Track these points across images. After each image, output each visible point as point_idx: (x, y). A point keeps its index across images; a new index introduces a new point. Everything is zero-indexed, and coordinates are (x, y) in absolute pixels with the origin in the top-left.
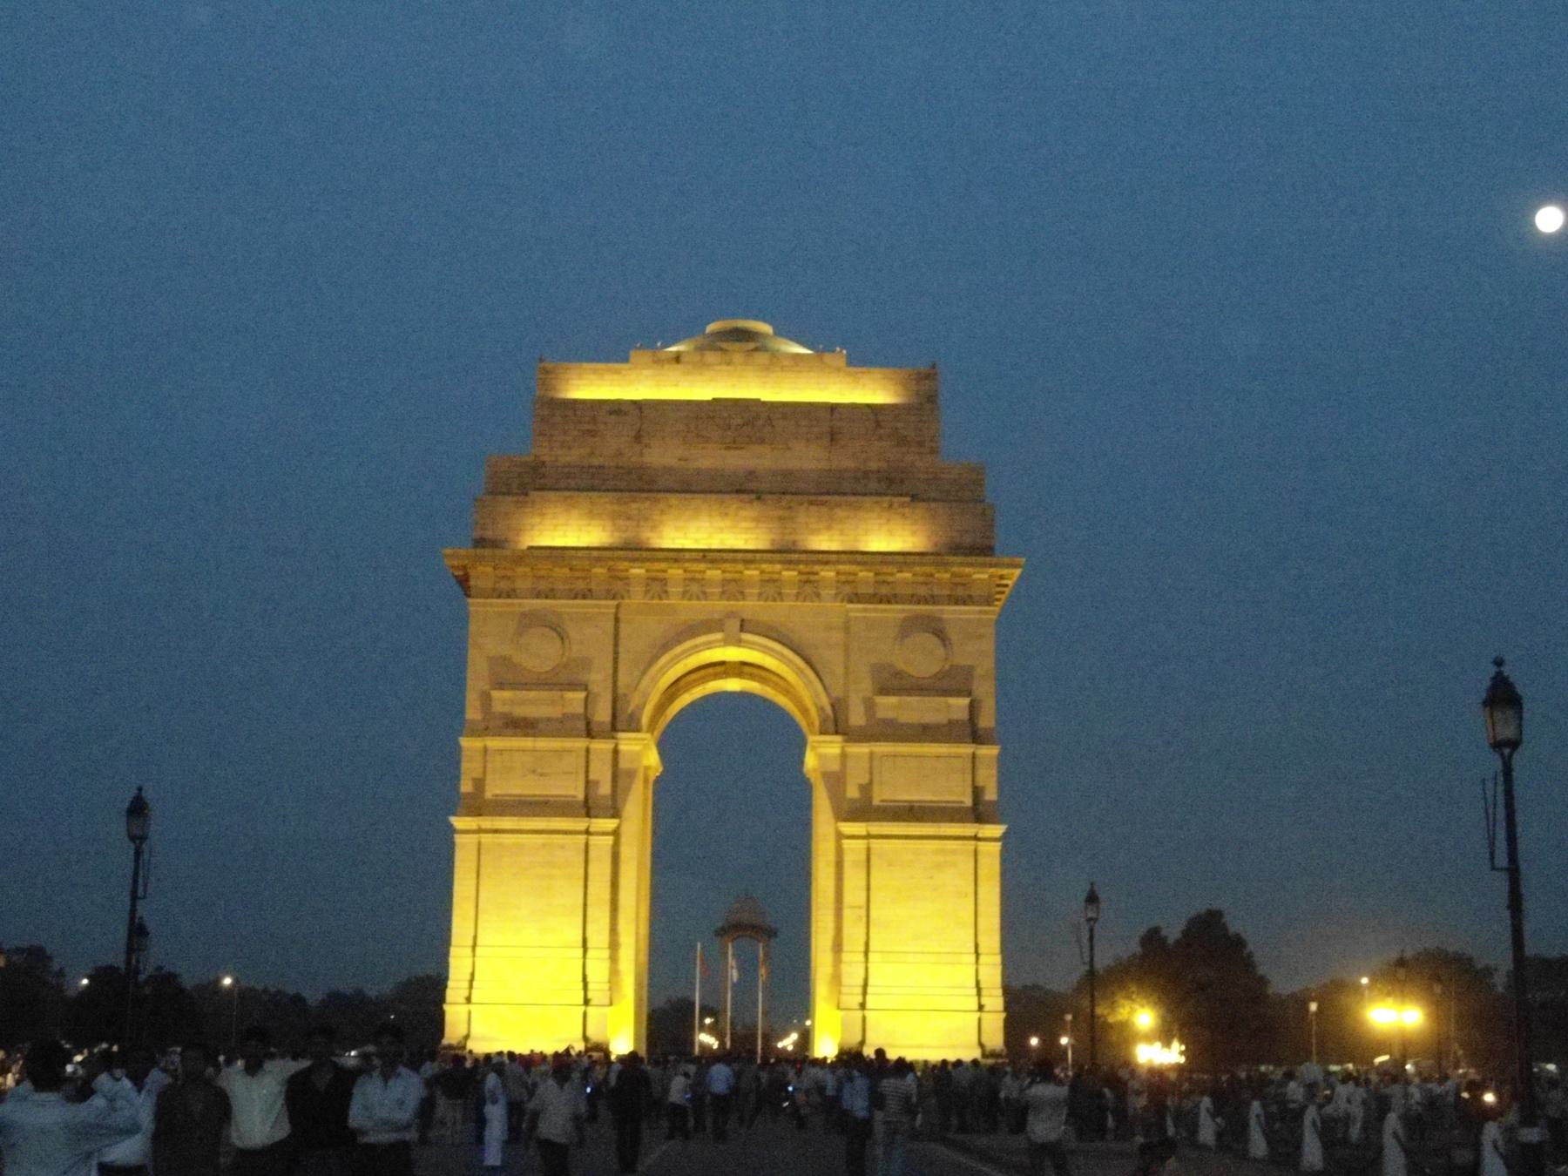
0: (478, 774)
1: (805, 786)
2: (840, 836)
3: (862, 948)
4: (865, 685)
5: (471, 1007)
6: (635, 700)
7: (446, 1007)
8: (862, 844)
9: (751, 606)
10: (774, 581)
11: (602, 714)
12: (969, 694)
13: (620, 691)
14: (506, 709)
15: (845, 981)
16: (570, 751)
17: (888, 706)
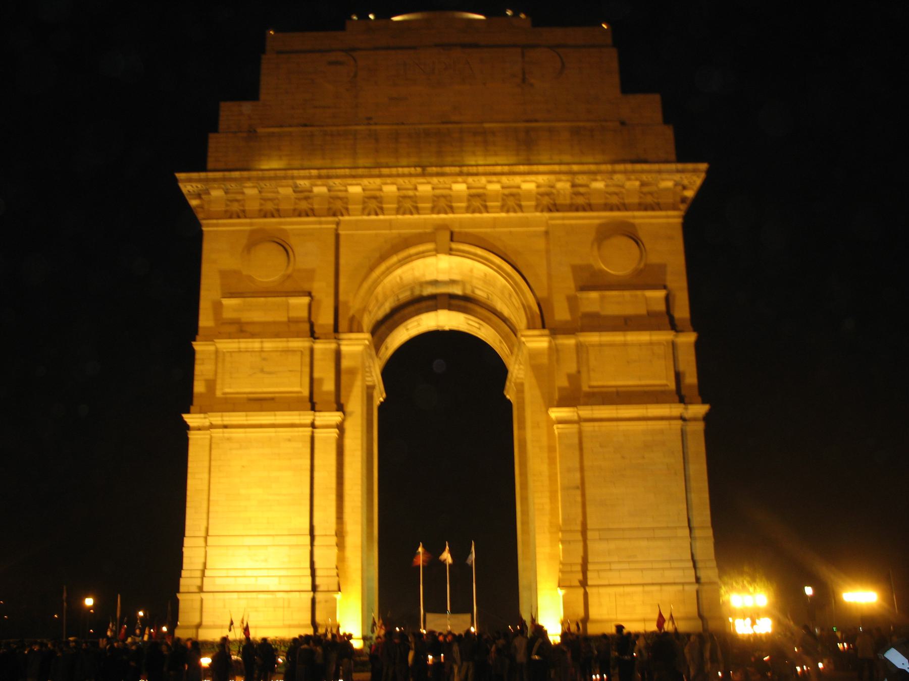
0: (210, 376)
3: (579, 528)
4: (566, 284)
5: (203, 595)
7: (180, 596)
8: (574, 428)
9: (459, 218)
10: (479, 196)
11: (325, 318)
12: (665, 287)
13: (342, 298)
17: (592, 300)
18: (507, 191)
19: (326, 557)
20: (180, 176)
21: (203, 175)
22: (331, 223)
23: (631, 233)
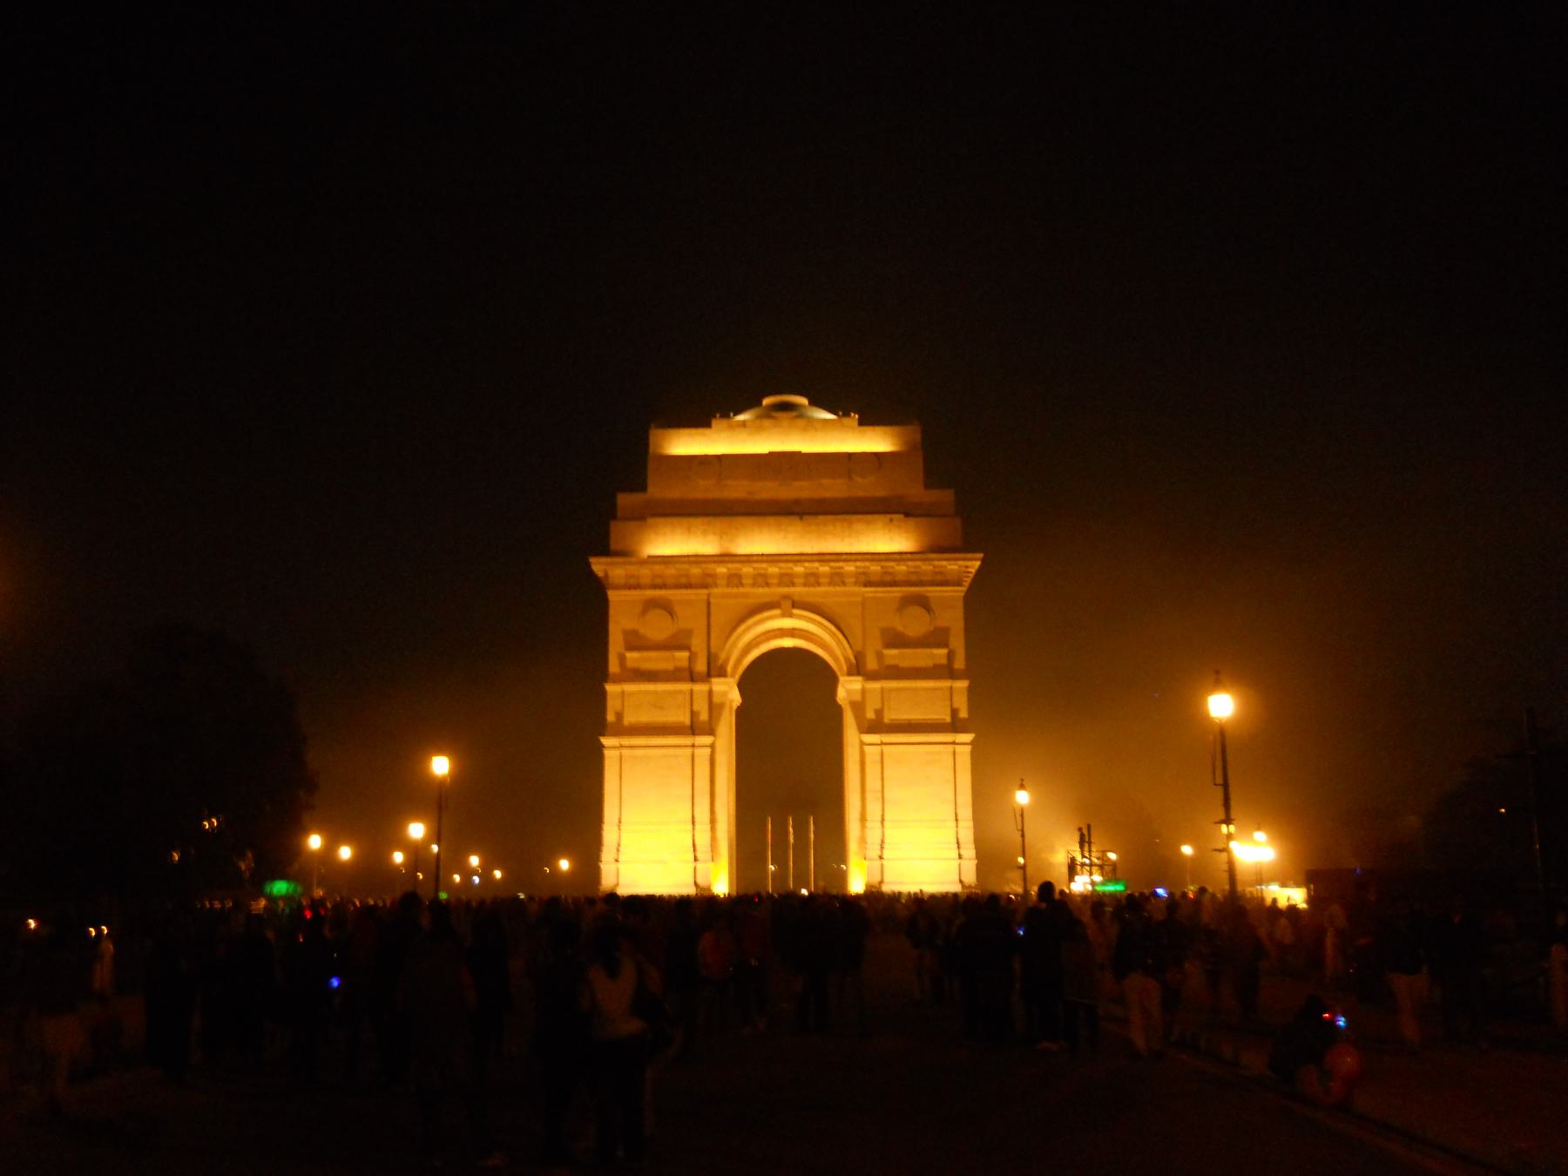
0: (619, 708)
1: (838, 711)
2: (862, 744)
6: (723, 656)
9: (798, 591)
11: (701, 666)
12: (945, 645)
13: (713, 650)
14: (635, 665)
15: (869, 840)
16: (680, 692)
17: (892, 654)
19: (703, 838)
20: (593, 560)
21: (609, 560)
23: (923, 603)
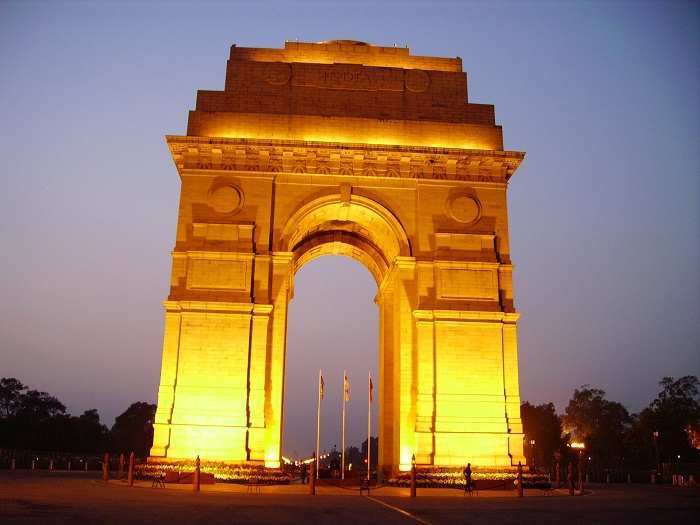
0: (183, 275)
2: (415, 321)
3: (431, 392)
7: (154, 425)
8: (430, 325)
13: (276, 227)
18: (391, 163)
22: (270, 176)
